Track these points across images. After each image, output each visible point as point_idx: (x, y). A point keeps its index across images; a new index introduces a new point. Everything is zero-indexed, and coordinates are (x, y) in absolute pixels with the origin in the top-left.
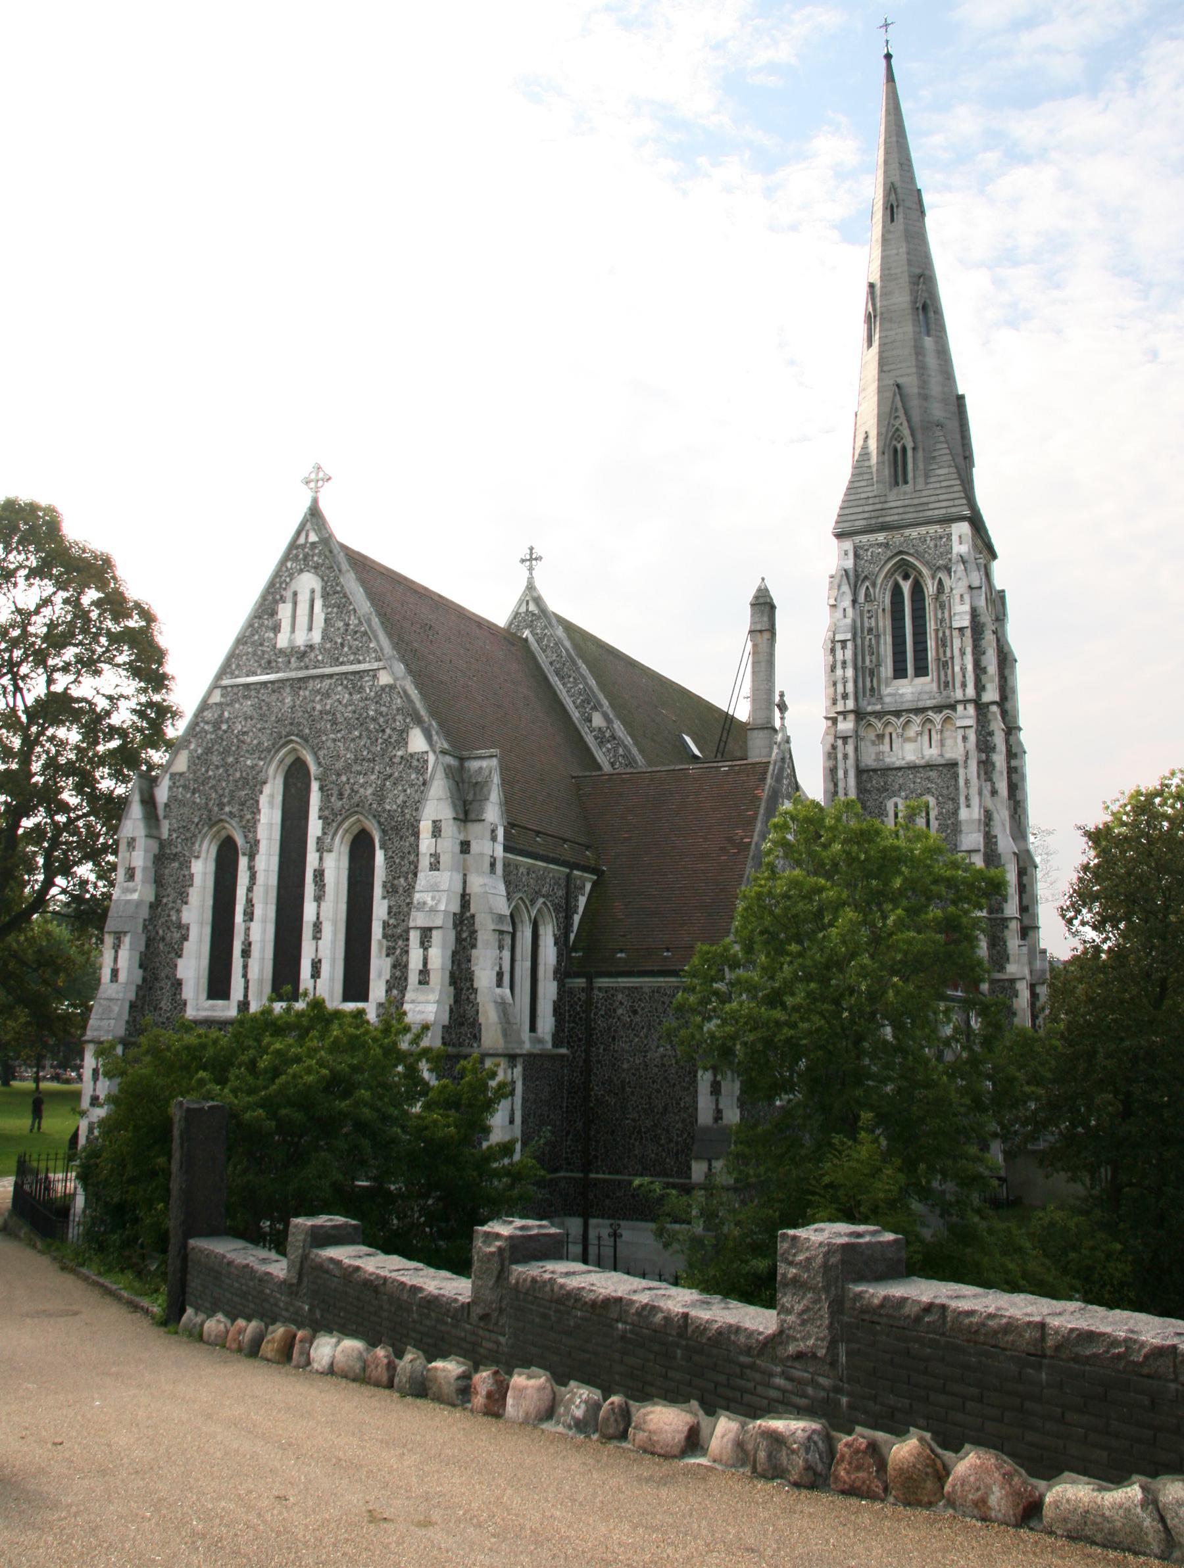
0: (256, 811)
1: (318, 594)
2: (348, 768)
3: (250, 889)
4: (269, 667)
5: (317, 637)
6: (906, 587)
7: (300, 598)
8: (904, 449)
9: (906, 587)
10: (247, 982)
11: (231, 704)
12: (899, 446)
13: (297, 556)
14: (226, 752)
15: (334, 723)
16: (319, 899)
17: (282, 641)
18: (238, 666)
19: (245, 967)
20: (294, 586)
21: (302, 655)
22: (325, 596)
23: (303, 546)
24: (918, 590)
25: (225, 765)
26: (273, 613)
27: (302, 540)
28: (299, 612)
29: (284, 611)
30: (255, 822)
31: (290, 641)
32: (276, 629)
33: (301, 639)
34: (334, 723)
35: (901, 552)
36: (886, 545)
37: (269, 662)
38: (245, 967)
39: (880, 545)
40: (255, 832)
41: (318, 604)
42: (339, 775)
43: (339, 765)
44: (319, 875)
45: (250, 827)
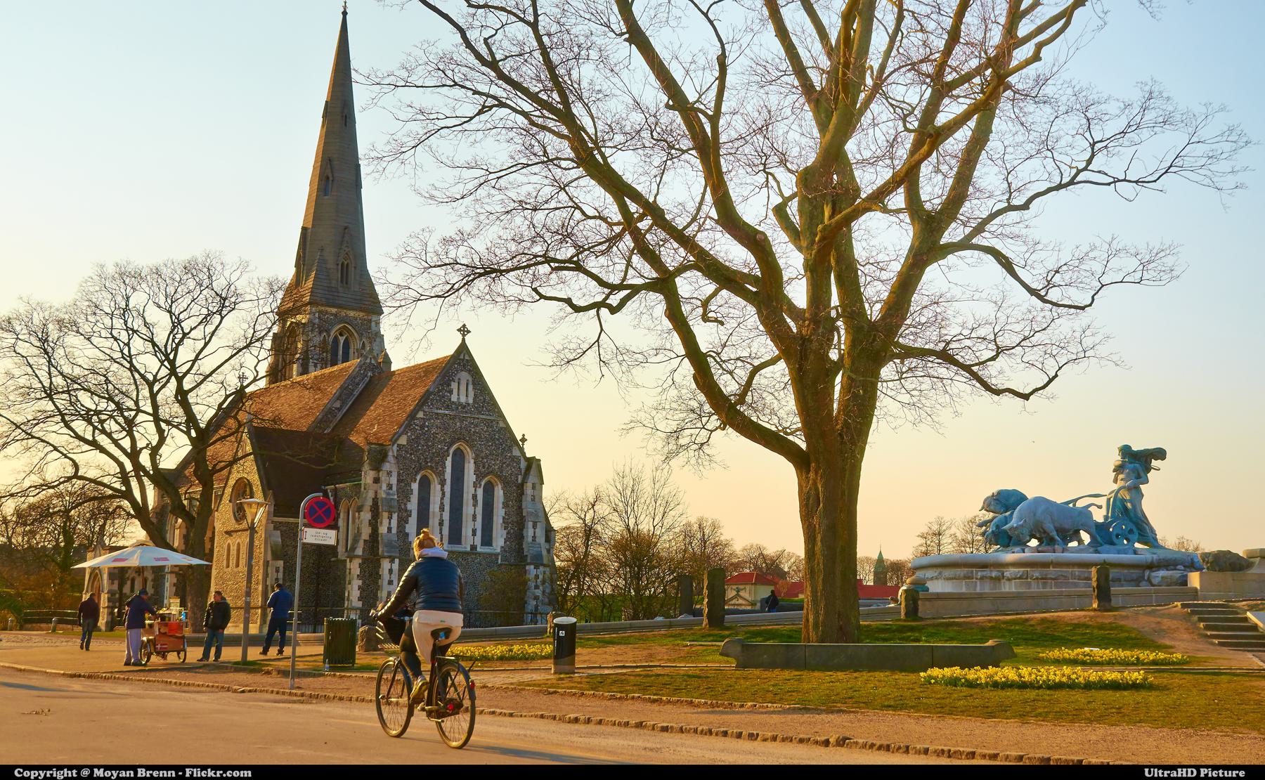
0: (444, 467)
1: (470, 383)
2: (487, 456)
3: (442, 499)
4: (447, 407)
5: (471, 401)
6: (342, 339)
7: (461, 382)
8: (347, 264)
9: (342, 339)
10: (442, 535)
11: (429, 420)
12: (346, 263)
13: (460, 363)
14: (427, 440)
15: (480, 437)
16: (475, 505)
17: (454, 398)
18: (432, 404)
19: (441, 530)
20: (459, 376)
21: (464, 407)
22: (474, 384)
23: (463, 360)
24: (346, 344)
25: (427, 446)
26: (449, 385)
27: (462, 357)
28: (461, 388)
29: (454, 386)
30: (444, 472)
31: (459, 399)
32: (451, 392)
33: (463, 400)
34: (480, 437)
35: (346, 323)
36: (336, 315)
37: (448, 406)
38: (441, 530)
39: (332, 314)
40: (444, 476)
41: (471, 387)
42: (483, 459)
43: (483, 455)
44: (475, 497)
45: (441, 474)
